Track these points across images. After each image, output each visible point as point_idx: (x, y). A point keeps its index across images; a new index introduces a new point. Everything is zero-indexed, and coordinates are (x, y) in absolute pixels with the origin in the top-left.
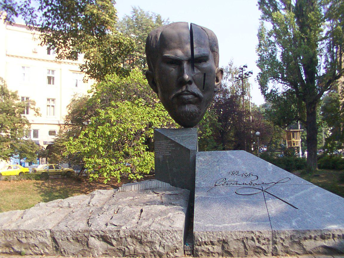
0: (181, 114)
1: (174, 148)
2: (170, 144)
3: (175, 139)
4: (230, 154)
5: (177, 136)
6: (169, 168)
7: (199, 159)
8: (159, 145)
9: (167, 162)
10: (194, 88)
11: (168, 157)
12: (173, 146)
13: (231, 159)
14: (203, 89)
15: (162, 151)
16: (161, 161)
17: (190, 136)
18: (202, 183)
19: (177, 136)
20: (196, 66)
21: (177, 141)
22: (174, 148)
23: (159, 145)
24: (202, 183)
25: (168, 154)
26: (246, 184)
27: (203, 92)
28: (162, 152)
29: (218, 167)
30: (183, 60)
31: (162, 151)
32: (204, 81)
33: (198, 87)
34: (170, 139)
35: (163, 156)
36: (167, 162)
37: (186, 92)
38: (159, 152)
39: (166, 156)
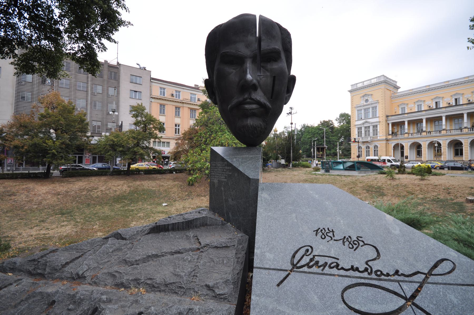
1: (231, 173)
2: (226, 168)
6: (224, 198)
7: (263, 195)
9: (223, 189)
10: (259, 96)
14: (271, 98)
15: (218, 174)
17: (252, 157)
21: (234, 165)
22: (231, 173)
24: (268, 255)
25: (224, 180)
26: (357, 269)
27: (270, 102)
28: (217, 175)
29: (294, 215)
31: (218, 174)
33: (265, 94)
34: (226, 161)
36: (223, 189)
37: (248, 100)
38: (215, 175)
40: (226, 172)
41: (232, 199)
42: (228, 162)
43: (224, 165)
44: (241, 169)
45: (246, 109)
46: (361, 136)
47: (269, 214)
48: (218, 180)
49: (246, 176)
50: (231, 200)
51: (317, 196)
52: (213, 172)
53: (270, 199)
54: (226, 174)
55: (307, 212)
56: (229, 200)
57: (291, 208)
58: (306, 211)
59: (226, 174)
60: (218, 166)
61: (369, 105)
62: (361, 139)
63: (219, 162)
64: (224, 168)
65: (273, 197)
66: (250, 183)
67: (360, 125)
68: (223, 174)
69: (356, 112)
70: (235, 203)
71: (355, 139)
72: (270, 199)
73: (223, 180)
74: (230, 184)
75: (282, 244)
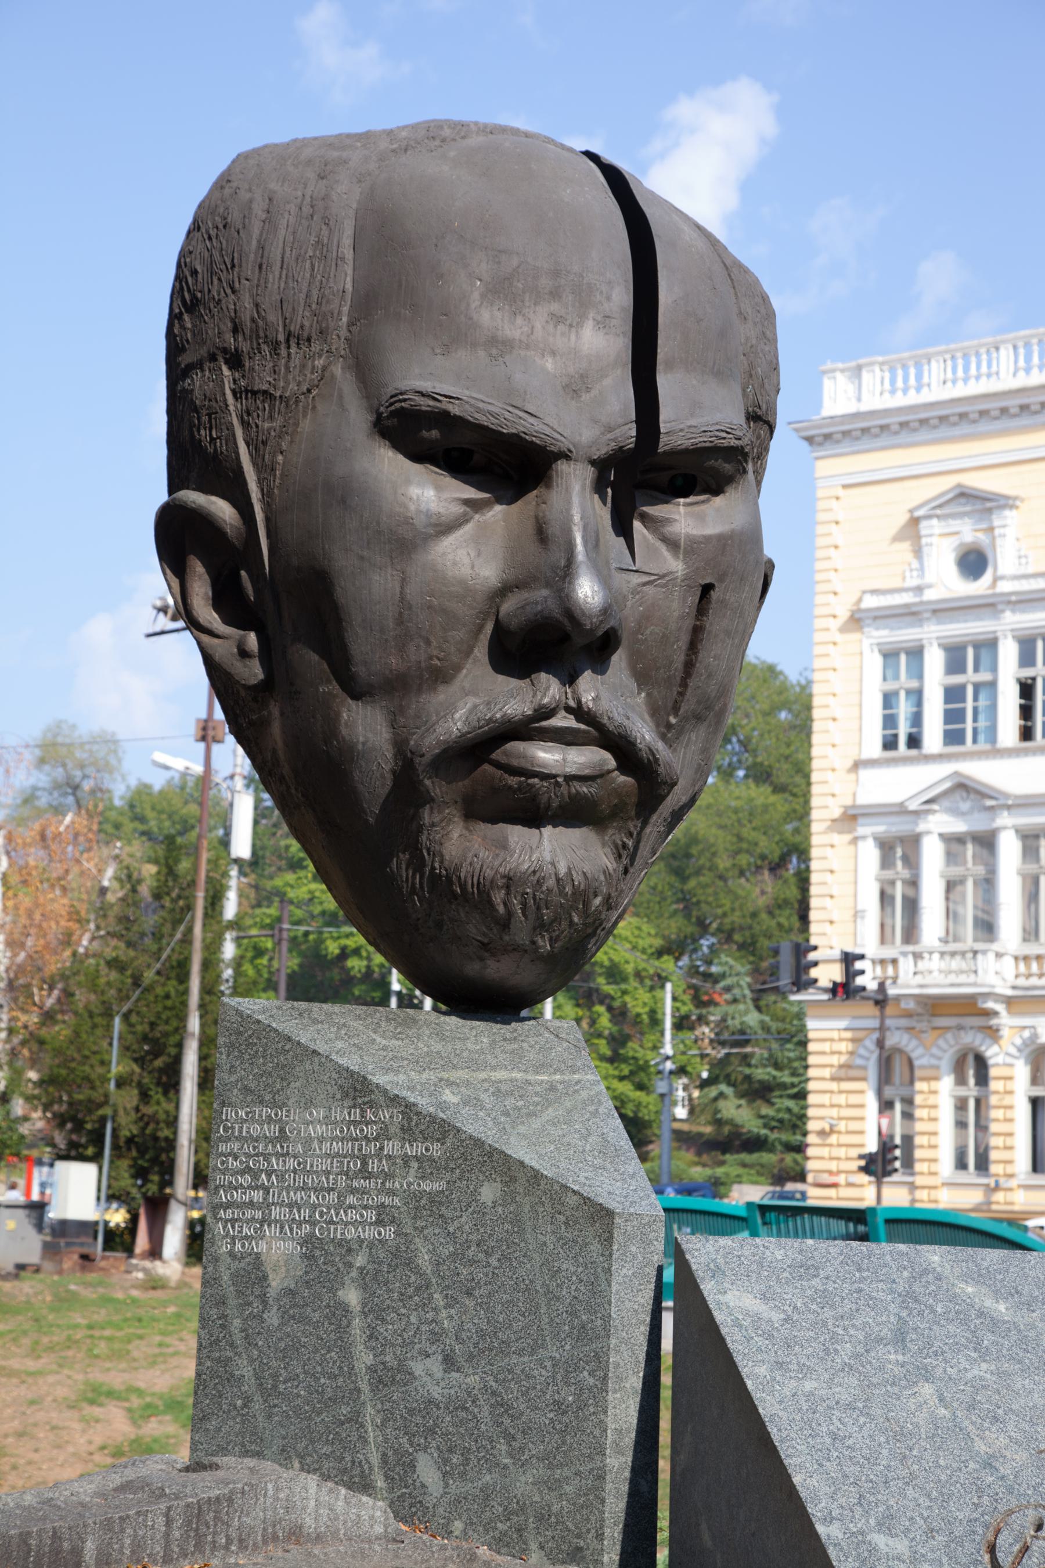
0: (498, 897)
3: (443, 1106)
4: (966, 1277)
5: (450, 1084)
6: (364, 1359)
8: (272, 1141)
9: (352, 1296)
11: (360, 1260)
12: (428, 1167)
13: (994, 1324)
15: (298, 1196)
16: (276, 1283)
18: (880, 1540)
19: (450, 1084)
20: (644, 518)
22: (436, 1186)
23: (272, 1141)
25: (370, 1233)
27: (665, 731)
30: (565, 456)
31: (298, 1196)
32: (693, 646)
35: (305, 1242)
36: (352, 1296)
37: (563, 721)
39: (347, 1248)
40: (388, 1176)
41: (449, 1362)
42: (408, 1108)
43: (371, 1131)
44: (519, 1150)
45: (545, 777)
46: (911, 933)
47: (809, 1385)
48: (305, 1242)
49: (572, 1200)
50: (437, 1369)
51: (1002, 1308)
52: (246, 1180)
53: (777, 1317)
54: (392, 1193)
55: (982, 1379)
56: (418, 1368)
57: (900, 1358)
58: (976, 1372)
59: (392, 1193)
60: (309, 1140)
61: (989, 606)
62: (906, 965)
63: (319, 1113)
64: (372, 1148)
65: (790, 1310)
66: (610, 1240)
67: (900, 810)
68: (353, 1191)
69: (875, 662)
70: (473, 1380)
71: (848, 959)
72: (777, 1317)
73: (351, 1233)
74: (424, 1259)
75: (924, 1501)
